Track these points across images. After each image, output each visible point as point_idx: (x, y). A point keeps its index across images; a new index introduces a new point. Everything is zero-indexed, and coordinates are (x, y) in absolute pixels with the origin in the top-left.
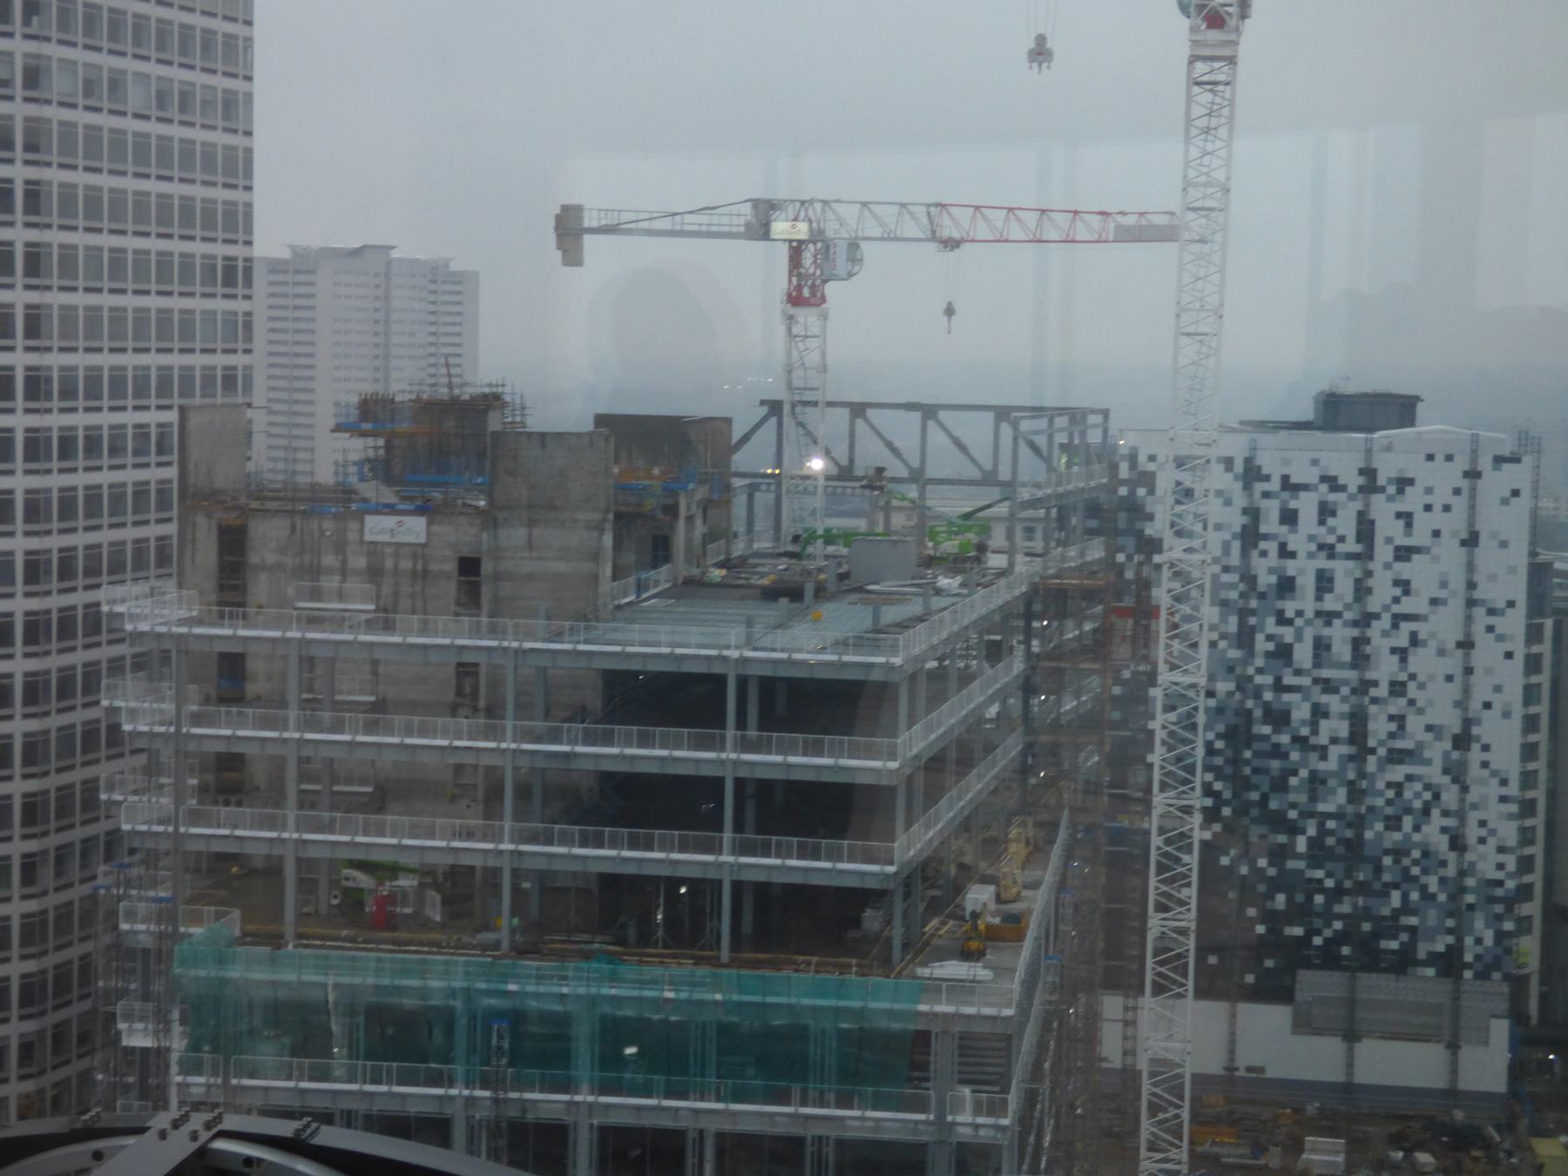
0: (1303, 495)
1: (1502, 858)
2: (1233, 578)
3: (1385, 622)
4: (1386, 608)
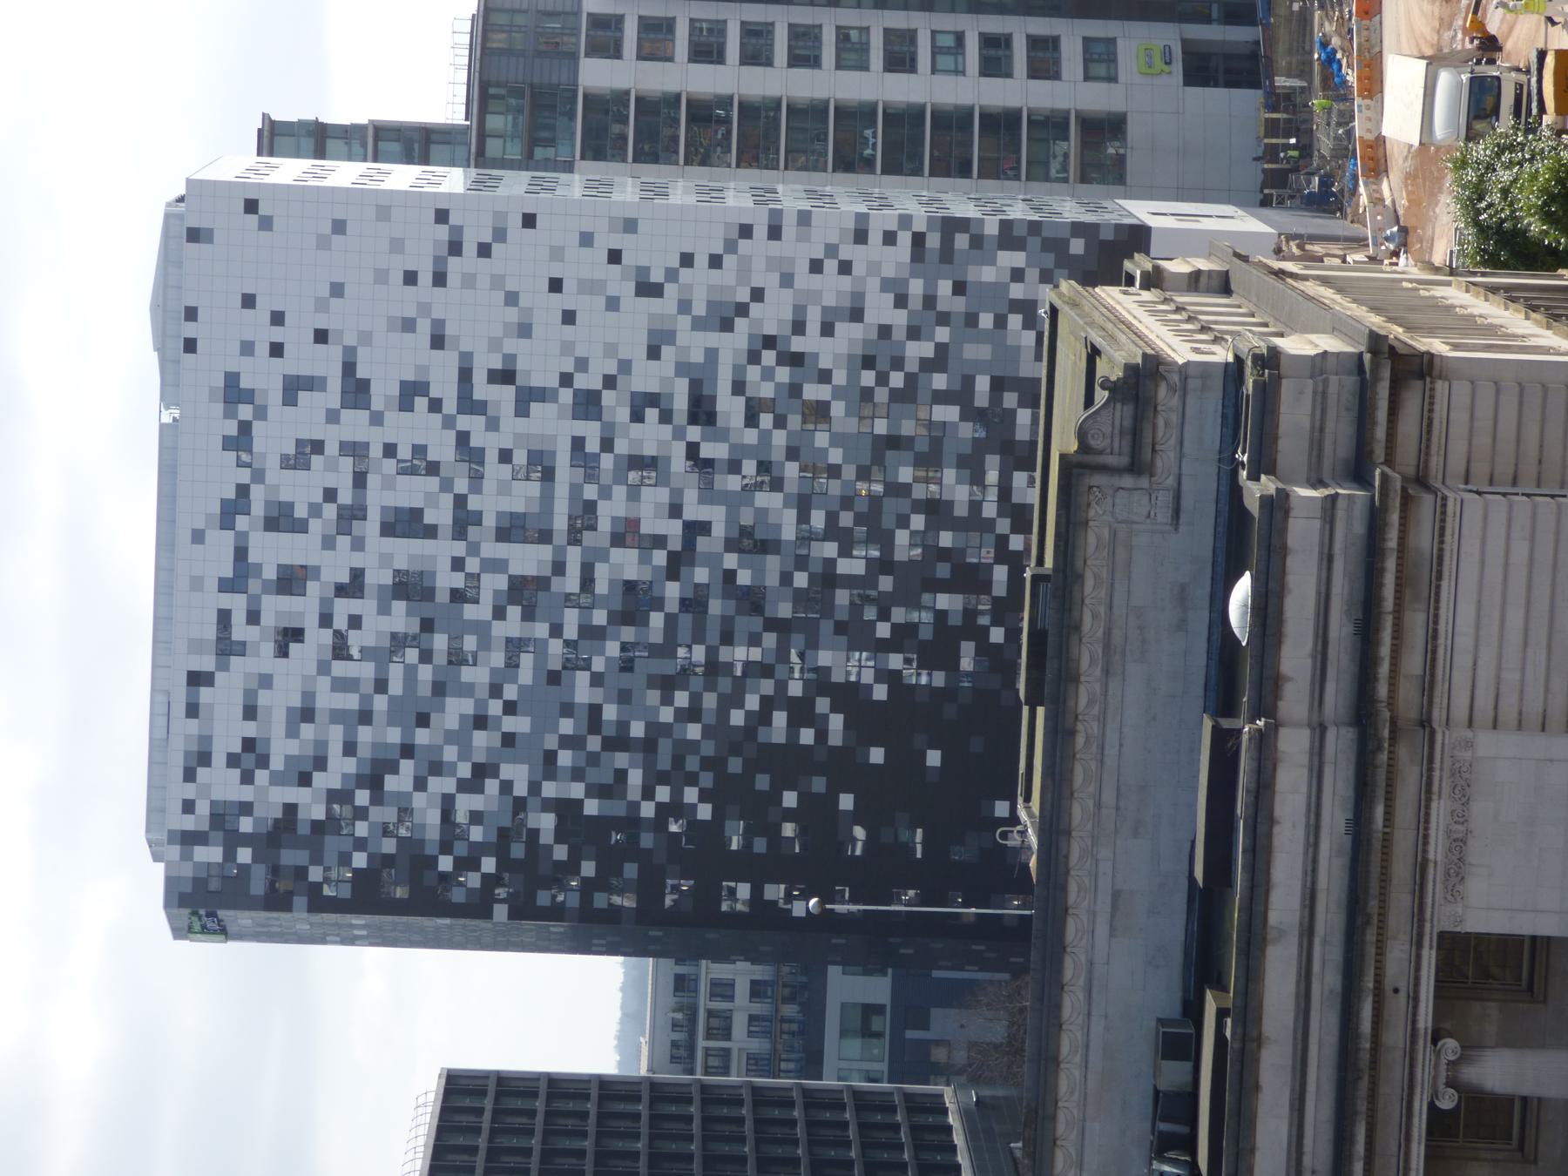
0: (253, 557)
1: (875, 237)
2: (396, 673)
3: (472, 424)
4: (449, 422)
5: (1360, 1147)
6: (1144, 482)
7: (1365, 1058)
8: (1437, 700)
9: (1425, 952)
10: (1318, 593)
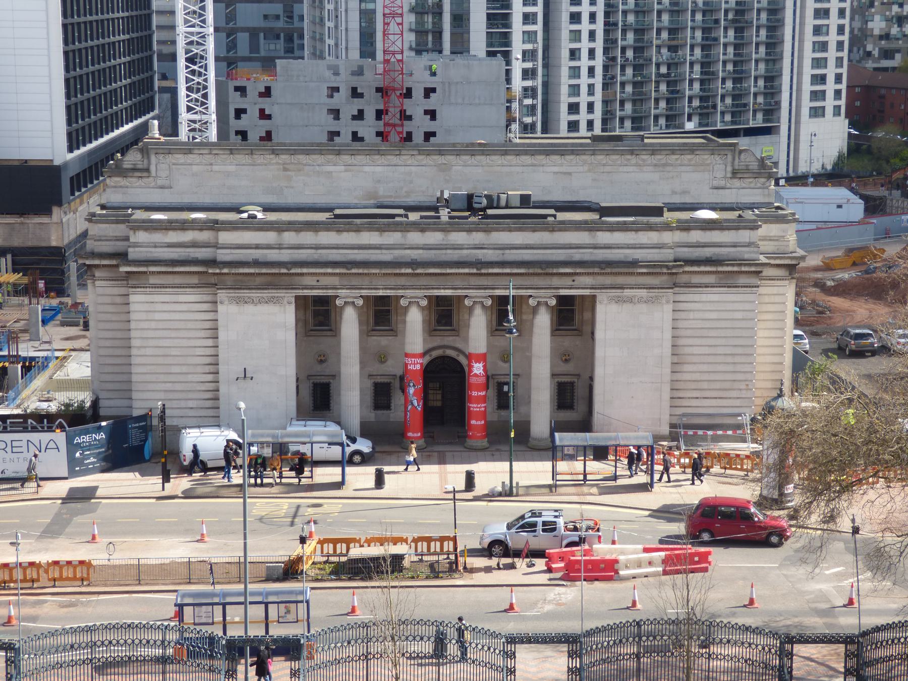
5: (515, 271)
6: (729, 175)
7: (550, 271)
8: (682, 289)
9: (589, 291)
10: (722, 243)
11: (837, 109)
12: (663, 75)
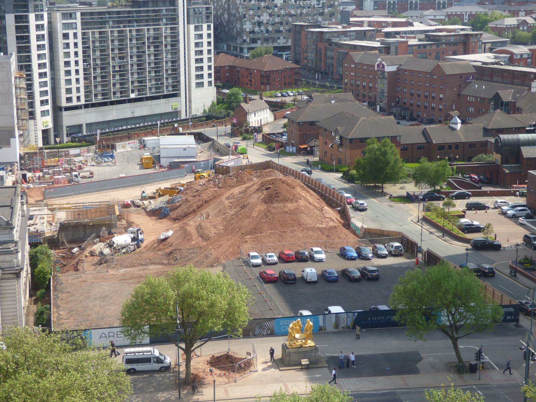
11: (210, 83)
12: (117, 71)
